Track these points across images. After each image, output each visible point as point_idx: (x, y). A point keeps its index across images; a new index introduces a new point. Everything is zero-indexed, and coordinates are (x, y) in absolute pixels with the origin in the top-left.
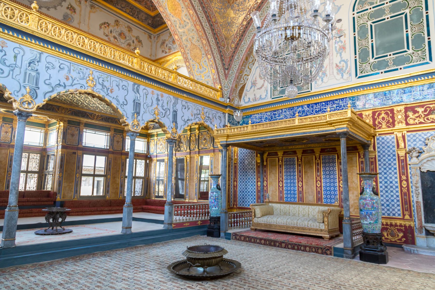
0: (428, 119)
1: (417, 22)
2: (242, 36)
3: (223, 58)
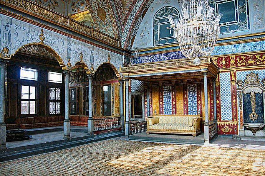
0: (247, 63)
1: (242, 5)
2: (134, 3)
3: (120, 18)
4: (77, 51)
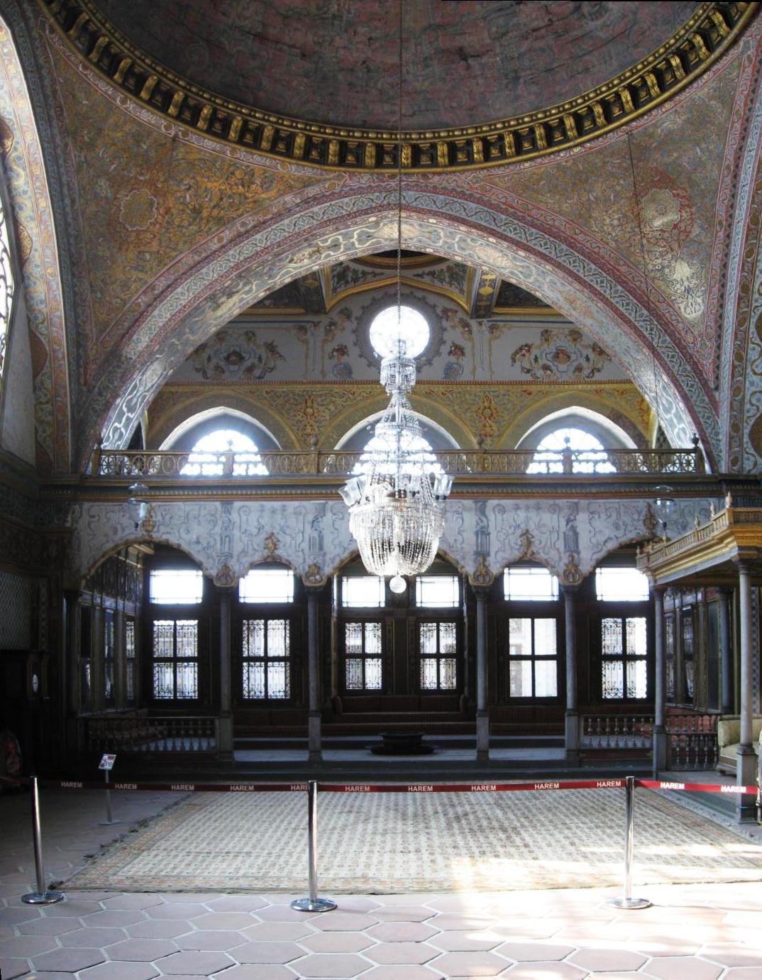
4: (510, 531)
